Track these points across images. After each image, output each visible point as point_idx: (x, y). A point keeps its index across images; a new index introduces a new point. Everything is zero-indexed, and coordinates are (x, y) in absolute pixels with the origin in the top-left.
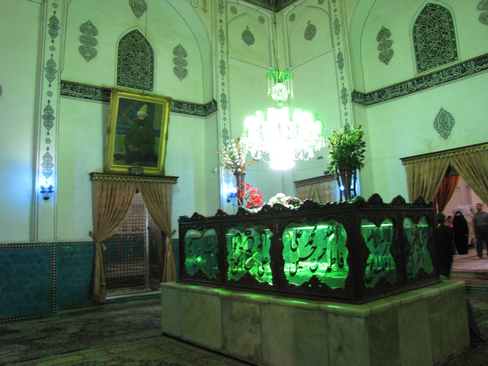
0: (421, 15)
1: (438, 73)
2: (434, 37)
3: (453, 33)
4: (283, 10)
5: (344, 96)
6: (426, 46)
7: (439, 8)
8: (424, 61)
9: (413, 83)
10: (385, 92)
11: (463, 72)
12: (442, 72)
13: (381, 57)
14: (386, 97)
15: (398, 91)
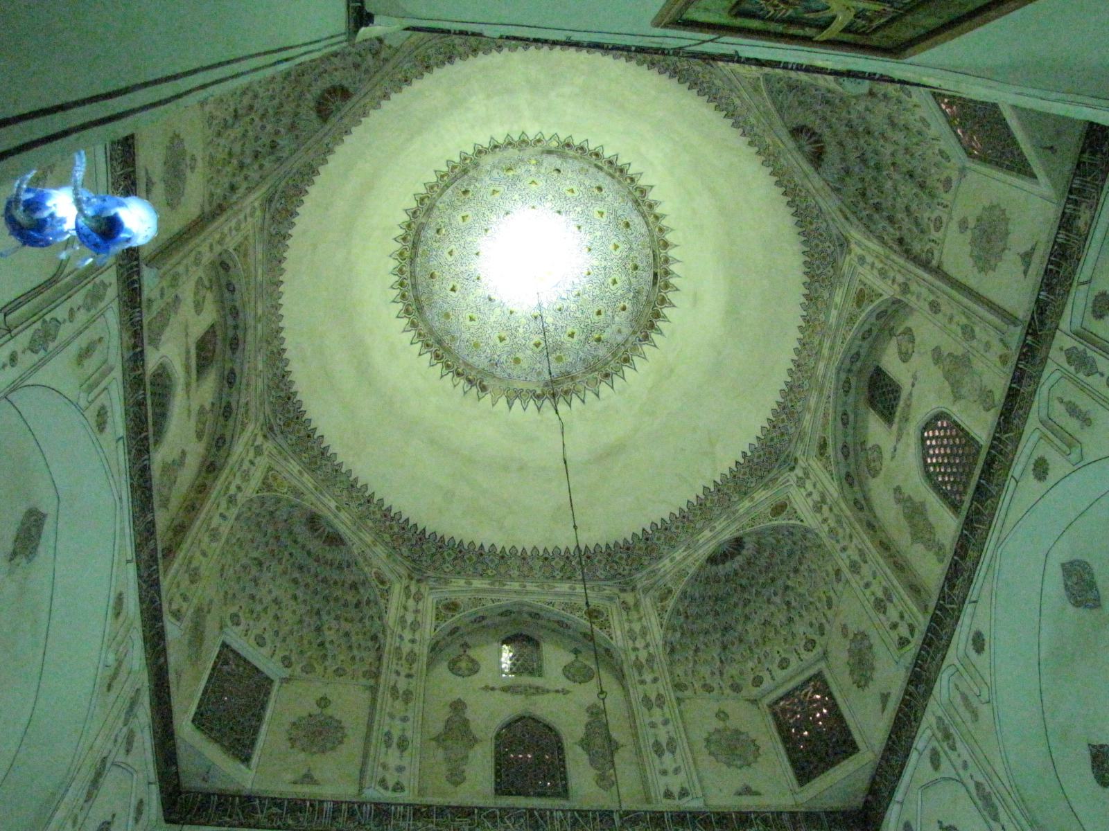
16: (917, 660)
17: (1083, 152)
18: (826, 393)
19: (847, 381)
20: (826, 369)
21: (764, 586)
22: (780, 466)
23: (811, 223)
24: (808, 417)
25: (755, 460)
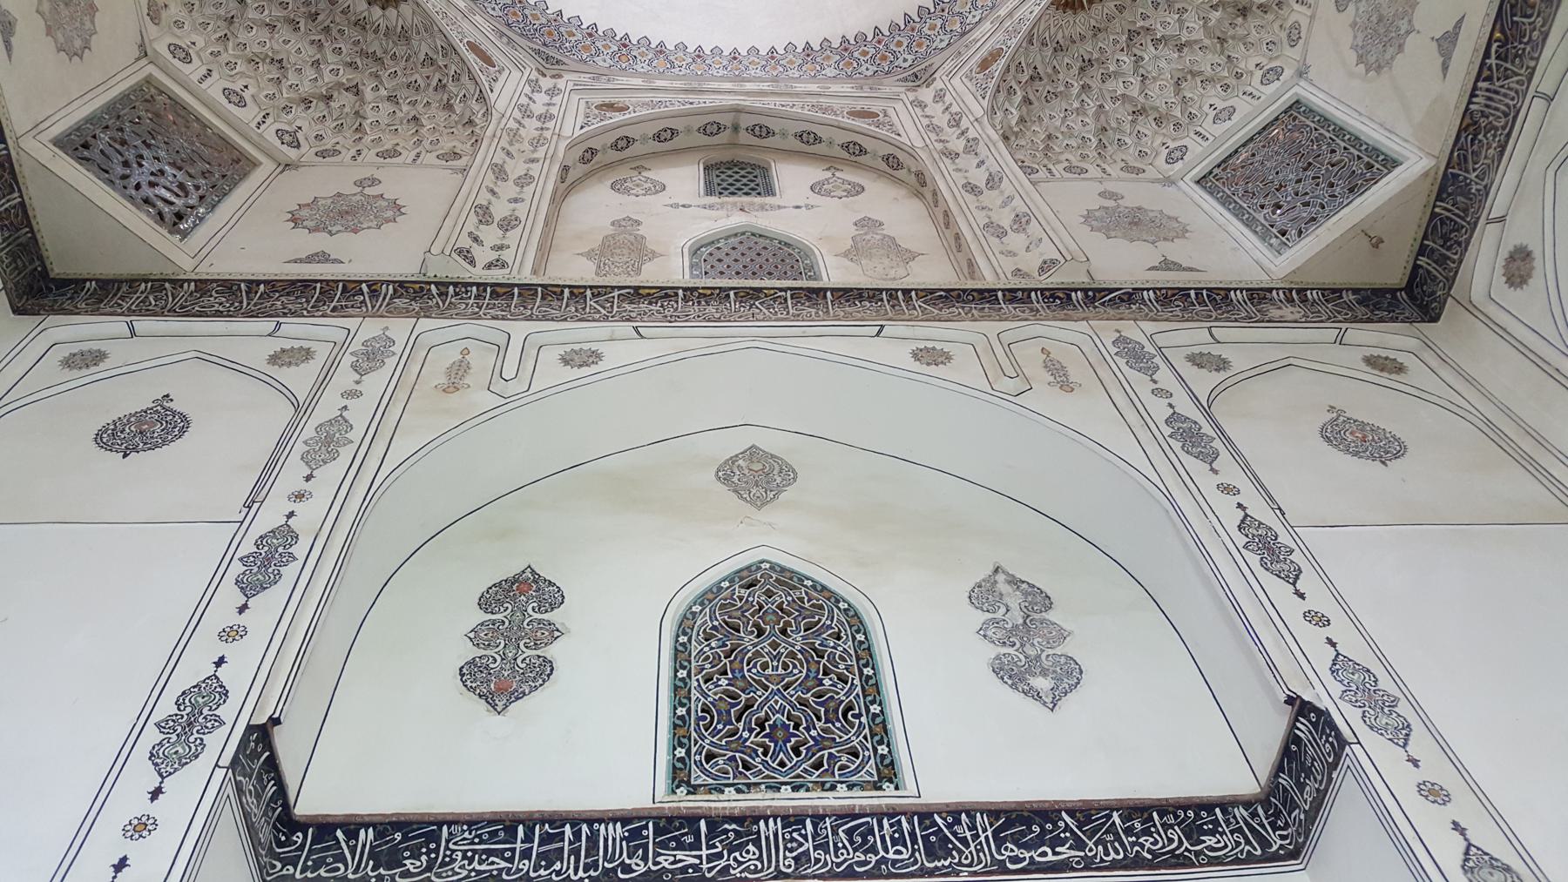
0: (725, 584)
1: (793, 820)
2: (780, 671)
3: (872, 689)
4: (53, 319)
5: (193, 714)
6: (734, 696)
7: (814, 587)
8: (710, 757)
9: (635, 834)
10: (434, 837)
11: (931, 854)
12: (818, 818)
13: (471, 674)
14: (429, 868)
15: (526, 854)
16: (455, 285)
17: (1355, 291)
18: (692, 97)
19: (720, 128)
20: (721, 95)
21: (338, 51)
22: (538, 52)
23: (932, 28)
24: (638, 82)
25: (527, 12)
